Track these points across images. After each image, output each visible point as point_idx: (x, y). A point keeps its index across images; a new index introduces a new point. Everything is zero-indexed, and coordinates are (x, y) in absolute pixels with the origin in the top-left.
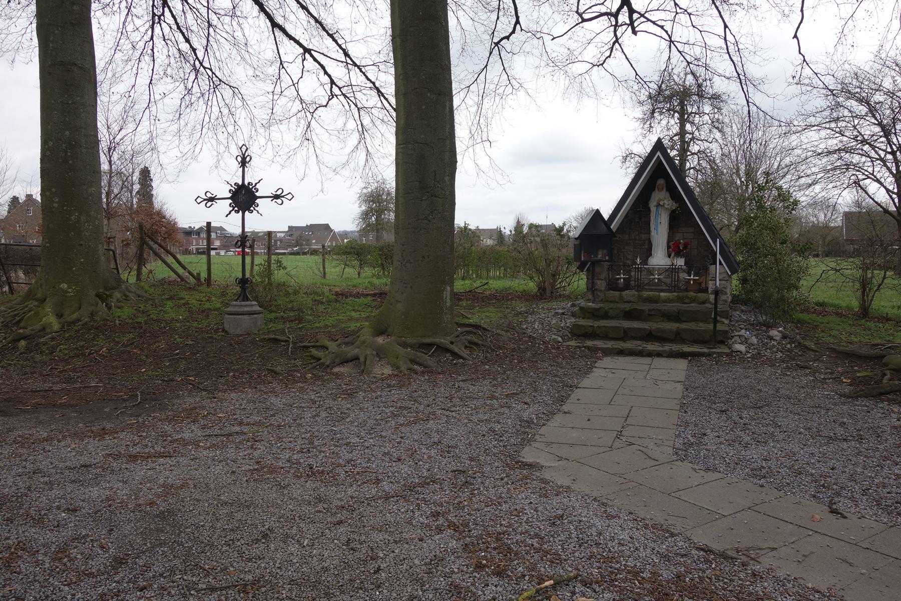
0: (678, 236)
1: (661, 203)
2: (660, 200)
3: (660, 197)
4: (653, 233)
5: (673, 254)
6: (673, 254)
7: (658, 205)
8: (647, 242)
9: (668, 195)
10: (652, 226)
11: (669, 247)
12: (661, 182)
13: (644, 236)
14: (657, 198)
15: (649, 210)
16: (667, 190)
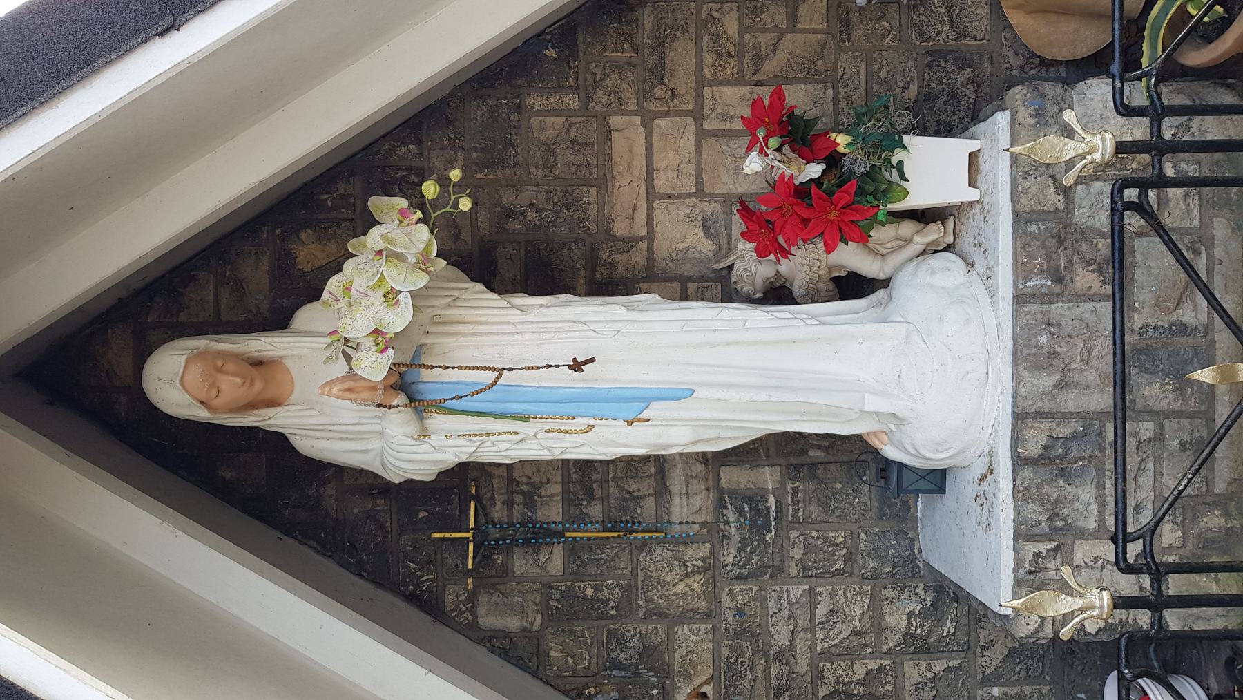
0: (680, 234)
1: (374, 366)
2: (351, 384)
3: (329, 383)
4: (672, 433)
5: (850, 257)
6: (850, 257)
7: (404, 387)
8: (730, 477)
9: (306, 316)
10: (609, 441)
11: (777, 294)
12: (177, 380)
13: (688, 505)
14: (348, 412)
15: (464, 478)
16: (279, 321)
